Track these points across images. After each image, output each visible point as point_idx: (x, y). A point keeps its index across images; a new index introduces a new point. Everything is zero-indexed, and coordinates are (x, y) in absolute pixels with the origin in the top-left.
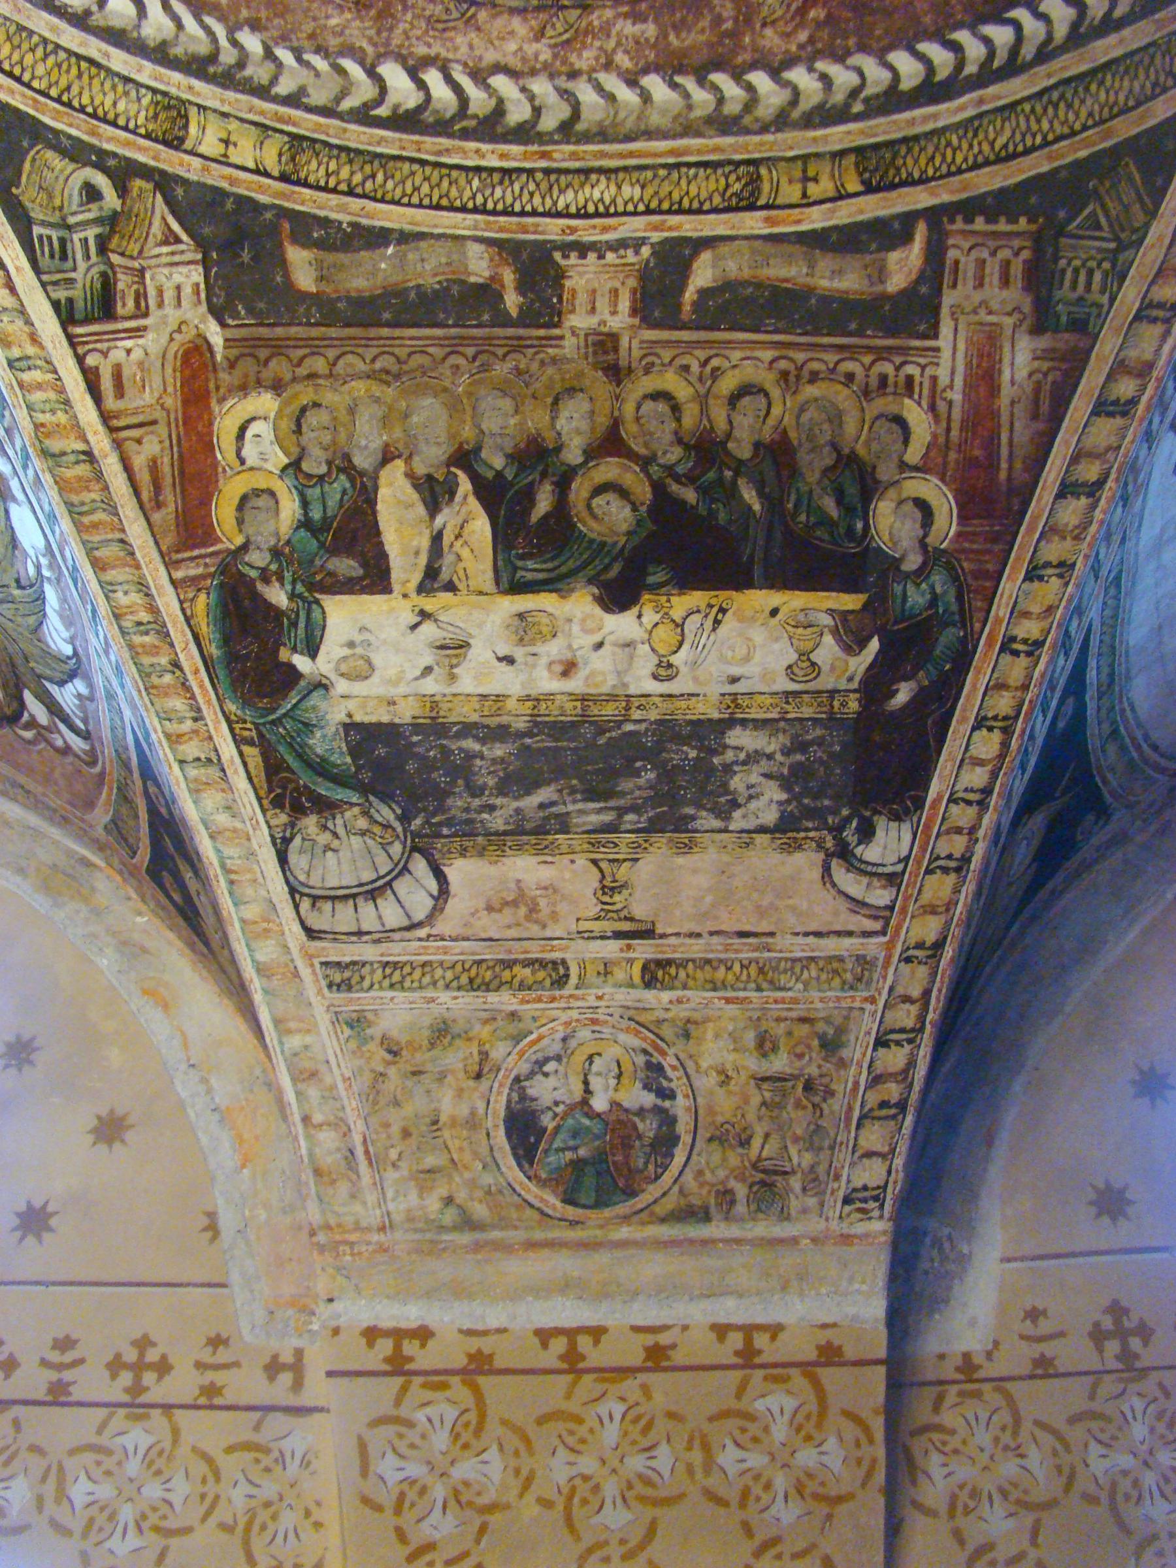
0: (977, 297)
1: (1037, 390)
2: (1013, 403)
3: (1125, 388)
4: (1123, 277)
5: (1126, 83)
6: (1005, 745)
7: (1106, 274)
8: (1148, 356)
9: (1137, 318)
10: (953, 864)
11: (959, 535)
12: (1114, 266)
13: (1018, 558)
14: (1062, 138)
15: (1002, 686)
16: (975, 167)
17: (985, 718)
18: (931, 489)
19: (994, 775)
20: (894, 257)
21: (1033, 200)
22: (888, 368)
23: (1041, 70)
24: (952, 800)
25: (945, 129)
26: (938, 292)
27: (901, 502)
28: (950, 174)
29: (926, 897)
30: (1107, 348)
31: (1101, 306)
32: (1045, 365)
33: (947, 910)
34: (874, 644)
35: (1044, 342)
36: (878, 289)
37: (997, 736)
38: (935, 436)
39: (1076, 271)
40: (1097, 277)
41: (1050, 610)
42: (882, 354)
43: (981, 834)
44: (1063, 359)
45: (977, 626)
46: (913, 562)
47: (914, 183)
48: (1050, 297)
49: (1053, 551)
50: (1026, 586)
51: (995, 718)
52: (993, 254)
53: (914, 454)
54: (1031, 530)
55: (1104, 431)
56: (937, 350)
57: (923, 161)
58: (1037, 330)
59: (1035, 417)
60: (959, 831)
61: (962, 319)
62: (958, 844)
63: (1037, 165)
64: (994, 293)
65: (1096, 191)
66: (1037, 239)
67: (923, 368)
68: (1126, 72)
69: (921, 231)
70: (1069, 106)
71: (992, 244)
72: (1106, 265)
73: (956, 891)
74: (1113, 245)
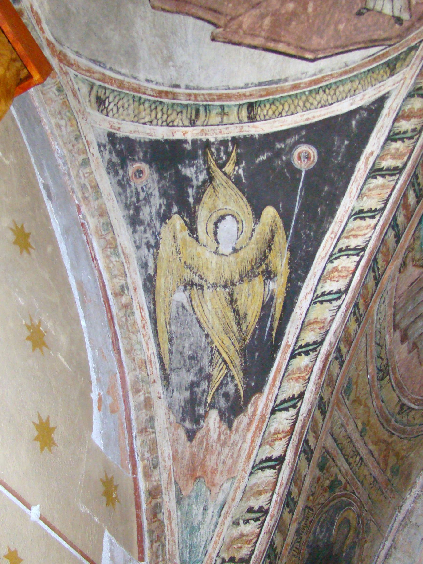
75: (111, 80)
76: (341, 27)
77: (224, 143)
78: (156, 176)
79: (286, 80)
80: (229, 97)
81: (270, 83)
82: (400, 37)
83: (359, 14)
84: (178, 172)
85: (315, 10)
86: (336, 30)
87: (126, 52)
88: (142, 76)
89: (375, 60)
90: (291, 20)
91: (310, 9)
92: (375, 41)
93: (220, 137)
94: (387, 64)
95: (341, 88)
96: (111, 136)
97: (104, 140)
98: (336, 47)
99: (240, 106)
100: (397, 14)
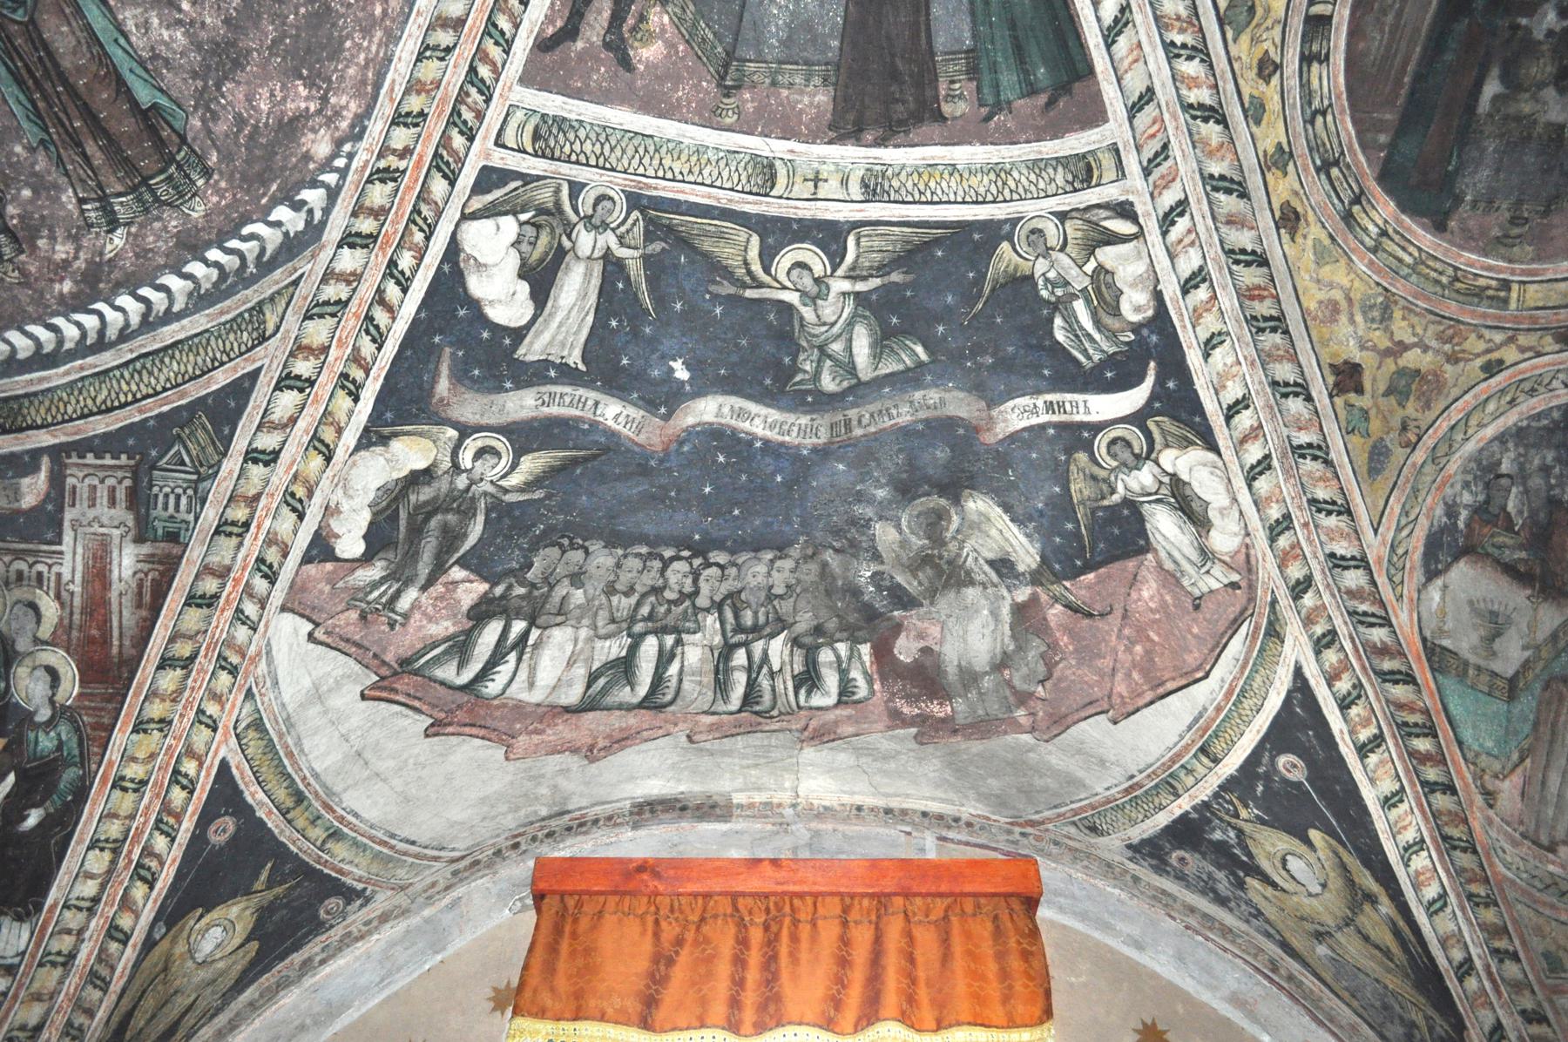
0: (91, 514)
1: (140, 586)
2: (121, 594)
3: (210, 585)
4: (204, 501)
5: (191, 358)
6: (113, 862)
7: (190, 497)
8: (227, 562)
9: (217, 532)
10: (60, 959)
11: (80, 695)
12: (196, 492)
13: (127, 715)
14: (148, 396)
15: (115, 816)
16: (83, 416)
17: (98, 841)
18: (56, 658)
19: (103, 887)
20: (26, 481)
21: (131, 442)
22: (23, 566)
23: (125, 346)
24: (66, 906)
25: (57, 387)
26: (61, 510)
27: (34, 668)
28: (64, 421)
29: (36, 985)
30: (196, 554)
31: (187, 523)
32: (146, 567)
33: (51, 998)
34: (11, 778)
35: (146, 549)
36: (16, 505)
37: (107, 856)
38: (61, 619)
39: (166, 496)
40: (184, 501)
41: (153, 756)
42: (19, 555)
43: (87, 935)
44: (160, 563)
45: (94, 767)
46: (44, 714)
47: (38, 427)
48: (148, 514)
49: (156, 710)
50: (135, 737)
51: (107, 841)
52: (102, 481)
53: (45, 631)
54: (136, 695)
55: (193, 618)
56: (61, 553)
57: (42, 411)
58: (139, 540)
59: (139, 606)
60: (69, 932)
61: (80, 530)
62: (66, 943)
63: (132, 416)
64: (103, 510)
65: (179, 436)
66: (135, 473)
67: (50, 566)
68: (190, 350)
69: (45, 463)
70: (150, 373)
71: (101, 474)
72: (190, 492)
73: (61, 982)
74: (194, 477)
75: (1083, 809)
76: (1195, 630)
77: (1216, 795)
78: (1197, 856)
79: (1205, 709)
80: (1179, 755)
81: (1196, 720)
82: (1252, 599)
83: (1197, 607)
84: (1210, 841)
85: (1159, 635)
86: (1195, 636)
87: (1068, 783)
88: (1099, 790)
89: (1254, 638)
90: (1152, 660)
91: (1156, 638)
92: (1235, 620)
93: (1209, 792)
94: (1267, 634)
95: (1255, 685)
96: (1129, 847)
97: (1130, 854)
98: (1212, 650)
99: (1195, 756)
100: (1226, 581)
